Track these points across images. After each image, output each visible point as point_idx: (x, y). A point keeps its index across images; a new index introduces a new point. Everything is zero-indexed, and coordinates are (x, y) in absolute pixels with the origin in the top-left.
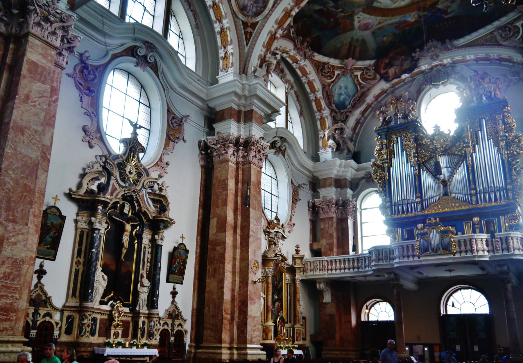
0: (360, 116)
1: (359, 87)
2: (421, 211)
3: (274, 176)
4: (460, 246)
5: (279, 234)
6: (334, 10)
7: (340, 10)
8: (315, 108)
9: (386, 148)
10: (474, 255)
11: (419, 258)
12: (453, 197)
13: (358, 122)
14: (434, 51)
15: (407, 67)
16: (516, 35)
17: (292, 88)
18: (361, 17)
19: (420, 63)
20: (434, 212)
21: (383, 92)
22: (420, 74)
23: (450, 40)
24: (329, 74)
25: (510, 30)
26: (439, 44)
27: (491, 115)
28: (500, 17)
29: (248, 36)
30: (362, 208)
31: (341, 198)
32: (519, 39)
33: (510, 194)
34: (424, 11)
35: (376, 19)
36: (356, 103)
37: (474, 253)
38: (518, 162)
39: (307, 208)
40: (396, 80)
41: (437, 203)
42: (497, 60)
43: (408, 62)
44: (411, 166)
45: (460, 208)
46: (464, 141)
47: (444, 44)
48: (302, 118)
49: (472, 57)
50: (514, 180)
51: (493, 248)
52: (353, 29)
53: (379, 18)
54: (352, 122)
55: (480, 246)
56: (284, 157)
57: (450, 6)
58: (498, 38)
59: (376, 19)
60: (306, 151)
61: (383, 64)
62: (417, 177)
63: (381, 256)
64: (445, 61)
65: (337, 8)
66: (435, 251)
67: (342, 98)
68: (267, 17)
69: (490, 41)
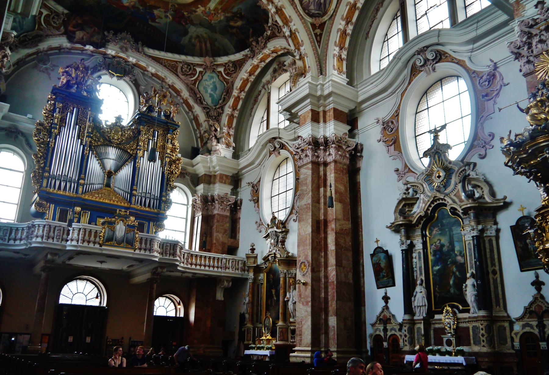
4: (141, 243)
9: (59, 112)
11: (101, 246)
12: (115, 191)
14: (125, 44)
15: (97, 41)
19: (108, 45)
21: (60, 49)
22: (102, 54)
23: (143, 45)
33: (163, 205)
34: (142, 6)
41: (97, 191)
44: (81, 144)
45: (119, 204)
46: (138, 143)
49: (153, 71)
57: (161, 18)
58: (179, 70)
63: (51, 234)
64: (131, 59)
66: (119, 243)
69: (172, 67)
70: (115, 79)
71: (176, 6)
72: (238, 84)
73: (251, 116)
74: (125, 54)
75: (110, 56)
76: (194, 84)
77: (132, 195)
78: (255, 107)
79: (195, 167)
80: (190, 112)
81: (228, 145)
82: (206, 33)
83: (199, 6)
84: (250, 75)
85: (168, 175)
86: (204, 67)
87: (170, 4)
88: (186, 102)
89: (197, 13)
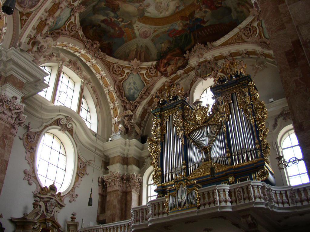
0: (147, 105)
1: (145, 83)
3: (62, 151)
5: (51, 200)
6: (116, 19)
7: (120, 19)
8: (109, 100)
9: (161, 125)
10: (216, 206)
15: (181, 65)
17: (89, 82)
19: (190, 61)
20: (196, 176)
23: (210, 43)
24: (119, 73)
25: (250, 29)
26: (203, 46)
27: (240, 90)
28: (242, 21)
29: (23, 22)
31: (126, 173)
32: (258, 36)
33: (259, 153)
36: (143, 96)
37: (217, 204)
38: (263, 125)
39: (97, 183)
40: (173, 76)
42: (246, 54)
43: (181, 61)
47: (206, 46)
48: (98, 107)
50: (262, 141)
51: (236, 198)
52: (135, 37)
53: (153, 27)
54: (139, 111)
55: (222, 196)
57: (205, 16)
58: (243, 36)
60: (100, 134)
61: (162, 64)
65: (117, 17)
67: (132, 91)
68: (39, 9)
69: (238, 40)
74: (202, 58)
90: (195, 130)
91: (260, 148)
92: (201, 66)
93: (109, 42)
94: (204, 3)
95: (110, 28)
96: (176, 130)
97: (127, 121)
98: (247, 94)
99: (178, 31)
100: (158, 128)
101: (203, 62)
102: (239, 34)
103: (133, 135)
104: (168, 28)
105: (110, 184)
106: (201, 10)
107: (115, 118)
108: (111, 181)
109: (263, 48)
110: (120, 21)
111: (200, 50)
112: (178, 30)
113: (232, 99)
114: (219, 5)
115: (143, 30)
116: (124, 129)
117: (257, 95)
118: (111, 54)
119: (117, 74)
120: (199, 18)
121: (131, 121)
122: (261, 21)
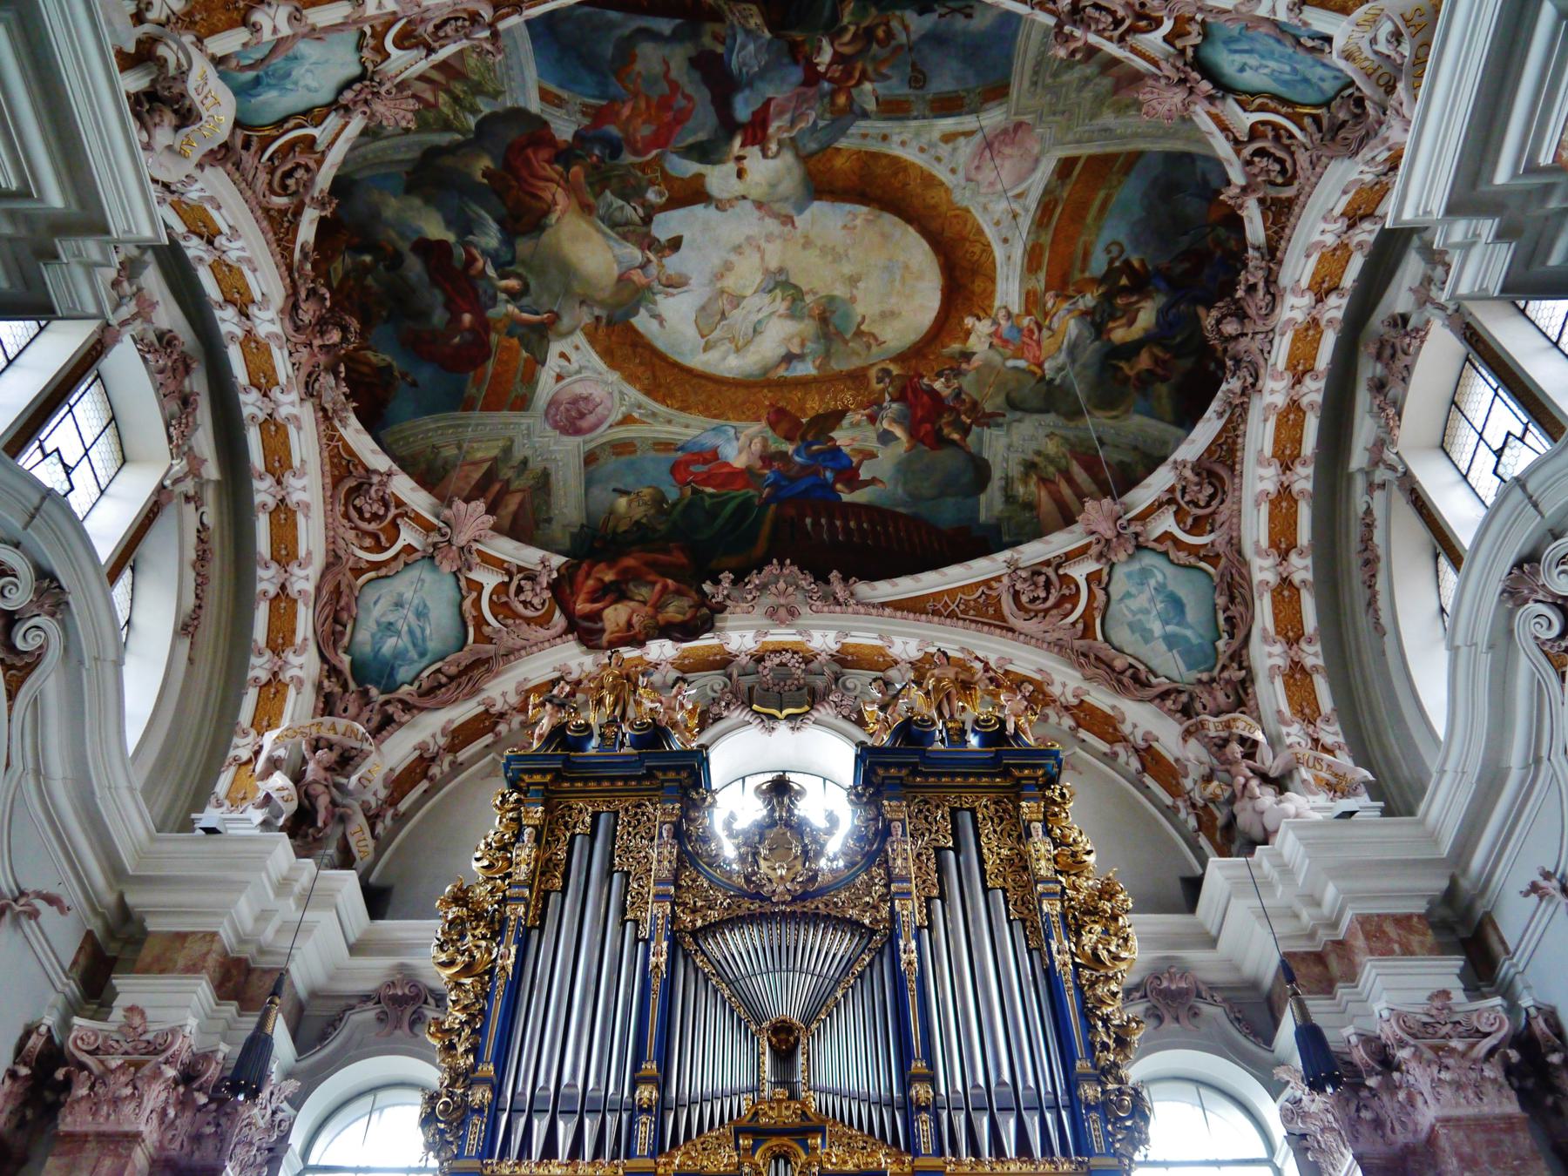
0: (442, 741)
1: (471, 630)
2: (652, 1155)
6: (491, 272)
7: (513, 283)
8: (260, 633)
9: (538, 840)
13: (421, 765)
14: (783, 593)
15: (680, 618)
16: (1068, 606)
18: (574, 356)
19: (725, 620)
23: (845, 579)
24: (373, 527)
25: (1048, 585)
26: (806, 581)
30: (312, 1161)
32: (1074, 624)
33: (1094, 1125)
34: (789, 438)
35: (621, 393)
43: (685, 603)
44: (636, 941)
46: (889, 873)
53: (634, 394)
54: (398, 749)
56: (11, 696)
57: (872, 455)
58: (1007, 605)
59: (621, 393)
62: (656, 984)
67: (389, 645)
70: (783, 728)
71: (895, 370)
72: (1255, 528)
73: (1383, 630)
74: (788, 626)
75: (744, 660)
76: (1088, 632)
77: (910, 1108)
78: (1380, 585)
79: (1222, 943)
80: (1119, 748)
81: (1337, 787)
82: (1050, 436)
83: (969, 321)
84: (1286, 467)
85: (1077, 975)
86: (1095, 550)
87: (873, 373)
88: (1086, 717)
89: (976, 361)
90: (734, 922)
91: (1105, 1108)
92: (768, 664)
93: (389, 366)
94: (900, 397)
95: (439, 297)
96: (627, 892)
97: (322, 774)
98: (1037, 827)
99: (725, 470)
100: (525, 854)
101: (779, 650)
102: (990, 588)
103: (332, 851)
104: (692, 433)
105: (100, 1090)
106: (872, 419)
107: (253, 733)
108: (120, 1067)
109: (1087, 679)
110: (506, 290)
111: (791, 589)
112: (727, 464)
113: (955, 834)
114: (956, 436)
115: (579, 389)
116: (294, 806)
117: (1089, 853)
118: (373, 422)
119: (356, 528)
120: (846, 450)
121: (344, 781)
122: (1112, 566)
